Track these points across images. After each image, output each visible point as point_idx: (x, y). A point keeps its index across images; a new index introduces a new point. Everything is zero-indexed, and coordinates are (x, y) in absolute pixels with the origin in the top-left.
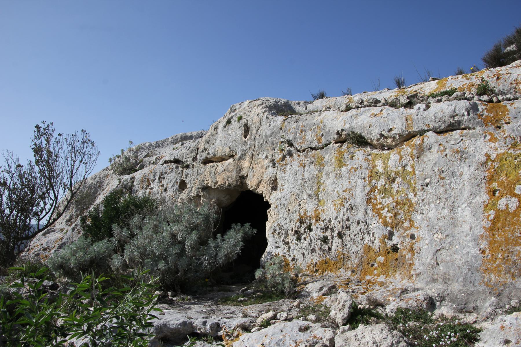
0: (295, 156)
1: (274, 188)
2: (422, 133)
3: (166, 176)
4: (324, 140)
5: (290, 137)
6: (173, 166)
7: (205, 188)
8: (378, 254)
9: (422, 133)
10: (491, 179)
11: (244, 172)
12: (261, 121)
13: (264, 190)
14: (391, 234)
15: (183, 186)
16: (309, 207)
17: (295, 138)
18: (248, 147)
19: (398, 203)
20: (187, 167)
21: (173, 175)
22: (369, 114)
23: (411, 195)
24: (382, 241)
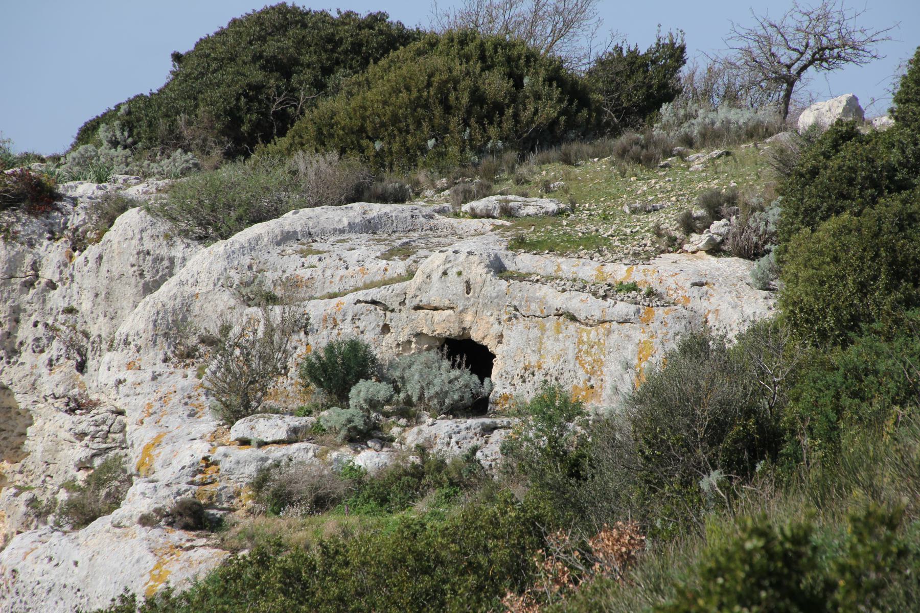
0: (521, 319)
1: (500, 342)
2: (610, 321)
3: (362, 317)
4: (545, 312)
5: (516, 303)
6: (372, 307)
7: (419, 335)
8: (582, 390)
9: (610, 321)
10: (640, 352)
11: (467, 325)
12: (484, 282)
13: (490, 344)
14: (590, 378)
15: (386, 329)
16: (533, 359)
17: (521, 305)
18: (471, 303)
19: (594, 361)
20: (393, 311)
21: (372, 317)
22: (578, 299)
23: (602, 357)
24: (585, 383)
